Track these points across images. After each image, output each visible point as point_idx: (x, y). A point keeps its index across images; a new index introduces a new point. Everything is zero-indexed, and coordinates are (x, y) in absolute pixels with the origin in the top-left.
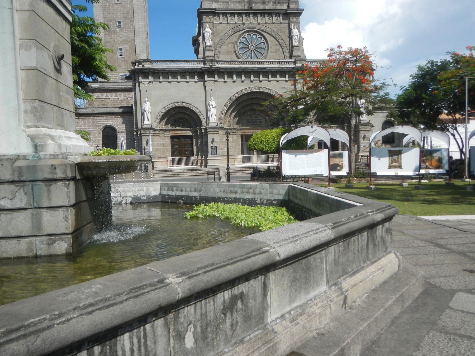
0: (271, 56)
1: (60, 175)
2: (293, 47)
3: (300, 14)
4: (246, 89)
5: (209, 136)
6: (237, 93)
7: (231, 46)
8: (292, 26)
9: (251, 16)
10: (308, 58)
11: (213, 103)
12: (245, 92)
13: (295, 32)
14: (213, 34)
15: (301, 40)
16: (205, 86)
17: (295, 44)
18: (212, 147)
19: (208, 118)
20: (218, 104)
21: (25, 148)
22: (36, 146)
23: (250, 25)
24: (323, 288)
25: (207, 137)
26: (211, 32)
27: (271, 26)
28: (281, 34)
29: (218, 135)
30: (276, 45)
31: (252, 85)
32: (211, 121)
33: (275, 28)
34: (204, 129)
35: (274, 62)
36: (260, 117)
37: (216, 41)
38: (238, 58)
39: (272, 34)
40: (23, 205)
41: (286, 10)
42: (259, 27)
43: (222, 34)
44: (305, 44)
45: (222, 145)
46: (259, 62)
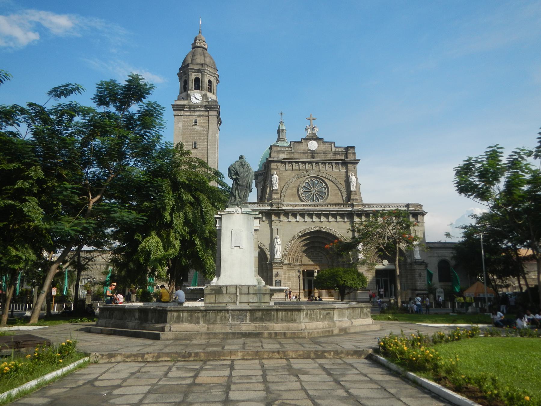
0: (331, 199)
1: (268, 292)
2: (351, 191)
3: (357, 163)
4: (308, 229)
5: (274, 270)
6: (300, 232)
7: (295, 190)
8: (350, 174)
9: (314, 164)
10: (364, 202)
11: (279, 240)
12: (307, 231)
13: (353, 178)
14: (279, 179)
15: (358, 185)
16: (271, 226)
17: (353, 189)
18: (276, 281)
19: (272, 255)
20: (283, 241)
21: (256, 283)
22: (259, 283)
23: (312, 172)
24: (346, 319)
25: (272, 272)
26: (278, 178)
27: (331, 173)
28: (339, 180)
29: (282, 270)
30: (336, 190)
31: (314, 225)
32: (276, 257)
33: (335, 175)
34: (269, 264)
35: (334, 205)
36: (321, 254)
37: (283, 186)
38: (302, 201)
39: (332, 180)
40: (256, 301)
41: (344, 160)
42: (321, 174)
43: (287, 180)
44: (361, 189)
45: (285, 279)
46: (320, 205)
